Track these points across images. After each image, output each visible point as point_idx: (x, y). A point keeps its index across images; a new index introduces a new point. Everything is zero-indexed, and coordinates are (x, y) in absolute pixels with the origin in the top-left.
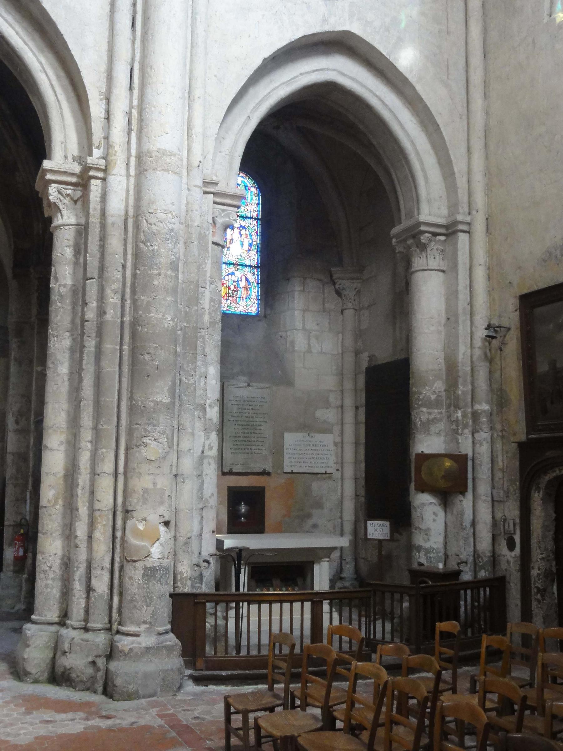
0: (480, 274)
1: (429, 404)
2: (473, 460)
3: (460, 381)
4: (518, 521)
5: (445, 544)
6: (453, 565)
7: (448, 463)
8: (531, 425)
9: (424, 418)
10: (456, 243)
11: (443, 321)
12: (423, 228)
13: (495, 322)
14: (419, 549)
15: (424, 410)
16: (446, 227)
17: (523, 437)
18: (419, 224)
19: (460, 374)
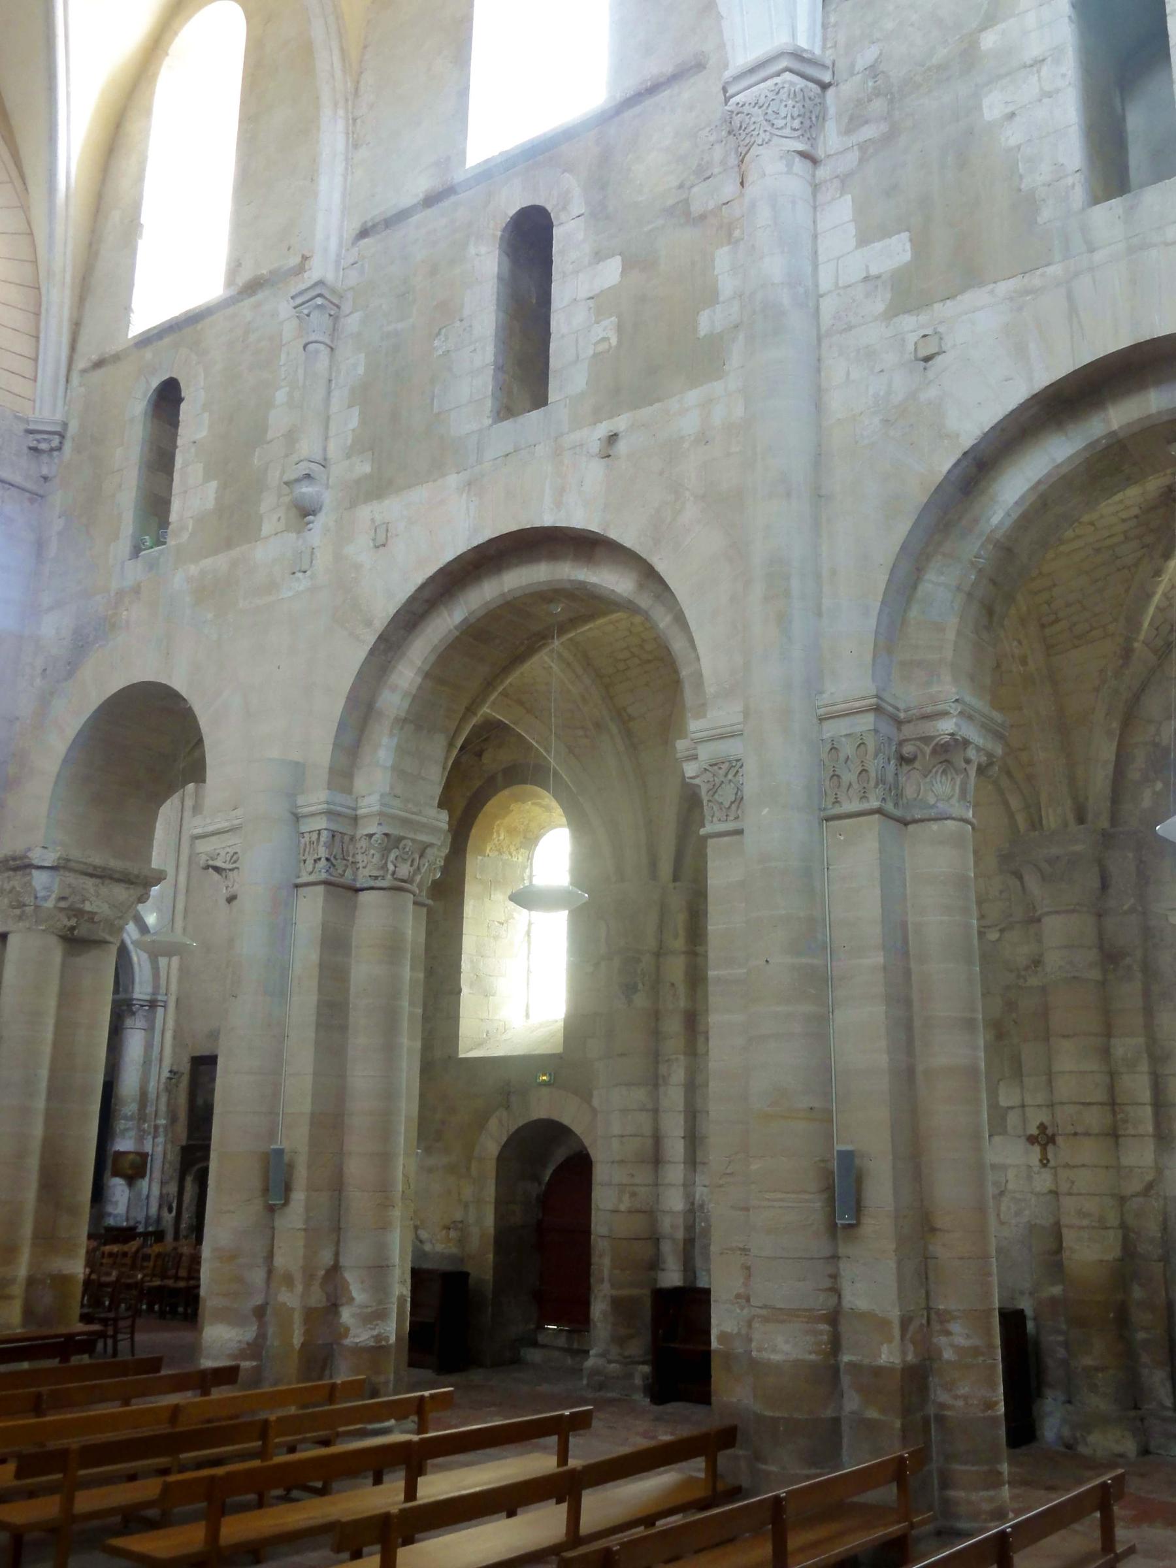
0: (169, 1035)
1: (126, 1118)
2: (152, 1154)
3: (149, 1104)
4: (176, 1194)
5: (128, 1212)
6: (132, 1223)
7: (131, 1157)
8: (189, 1137)
9: (122, 1127)
10: (155, 1013)
11: (142, 1062)
12: (135, 1002)
13: (175, 1069)
14: (110, 1214)
15: (123, 1122)
16: (150, 1001)
17: (184, 1143)
18: (133, 999)
19: (149, 1099)
